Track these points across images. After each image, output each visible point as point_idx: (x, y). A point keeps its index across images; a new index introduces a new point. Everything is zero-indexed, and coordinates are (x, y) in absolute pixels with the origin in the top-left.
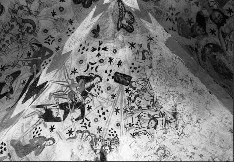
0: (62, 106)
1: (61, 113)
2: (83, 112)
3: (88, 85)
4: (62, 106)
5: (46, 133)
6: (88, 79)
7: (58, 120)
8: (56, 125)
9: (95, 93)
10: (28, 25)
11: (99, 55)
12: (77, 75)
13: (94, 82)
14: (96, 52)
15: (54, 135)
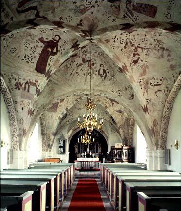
0: (134, 55)
1: (137, 56)
2: (140, 48)
3: (129, 44)
4: (134, 55)
5: (142, 64)
6: (127, 44)
7: (139, 58)
8: (141, 59)
9: (134, 41)
10: (100, 54)
11: (117, 39)
12: (123, 49)
13: (128, 41)
14: (116, 40)
15: (144, 61)
